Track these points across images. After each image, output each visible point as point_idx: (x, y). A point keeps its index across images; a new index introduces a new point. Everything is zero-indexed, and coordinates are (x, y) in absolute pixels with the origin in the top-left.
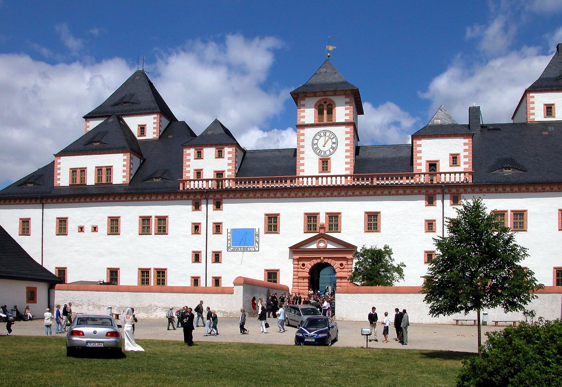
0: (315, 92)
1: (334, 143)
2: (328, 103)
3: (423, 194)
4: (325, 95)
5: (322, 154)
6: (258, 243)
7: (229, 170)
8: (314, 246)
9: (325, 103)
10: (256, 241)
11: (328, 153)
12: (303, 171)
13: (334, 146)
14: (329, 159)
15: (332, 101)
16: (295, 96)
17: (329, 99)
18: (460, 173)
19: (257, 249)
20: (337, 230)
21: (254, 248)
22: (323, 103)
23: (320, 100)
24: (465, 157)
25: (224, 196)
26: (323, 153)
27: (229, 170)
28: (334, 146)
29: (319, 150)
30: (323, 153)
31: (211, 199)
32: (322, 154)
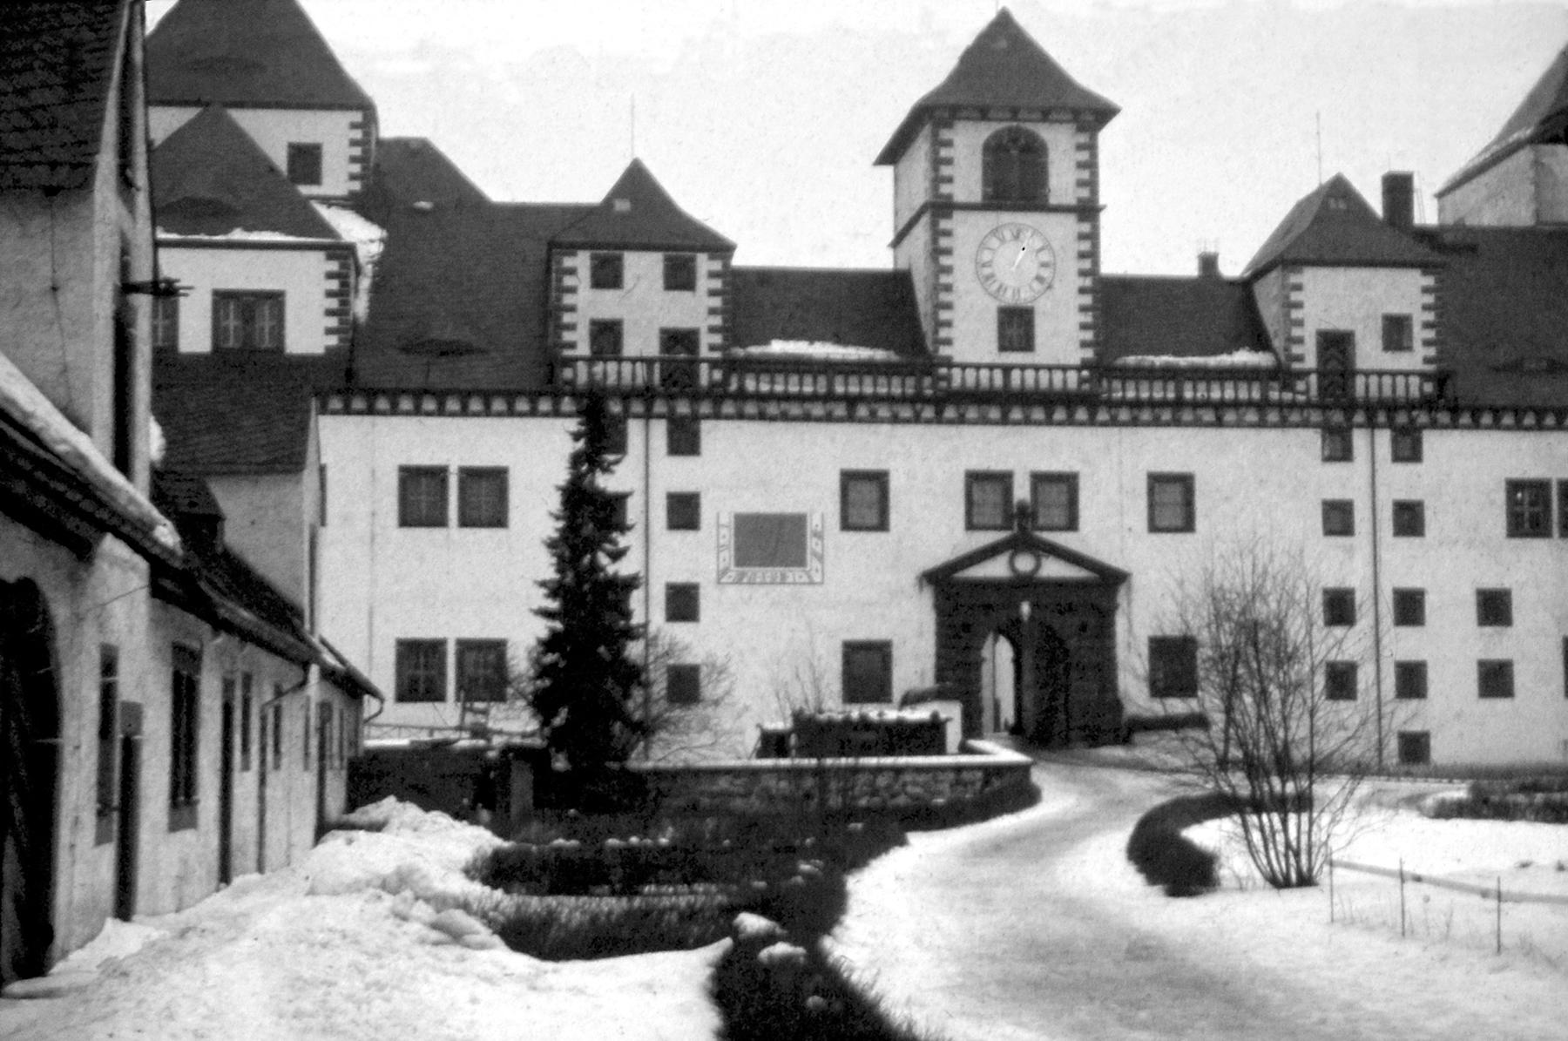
1: (1044, 265)
3: (1315, 426)
5: (1009, 294)
6: (821, 558)
7: (712, 330)
8: (996, 569)
10: (815, 554)
13: (1046, 273)
18: (1407, 374)
19: (817, 578)
20: (1072, 524)
21: (809, 577)
24: (1427, 325)
25: (705, 408)
27: (712, 330)
31: (660, 416)
32: (1009, 294)
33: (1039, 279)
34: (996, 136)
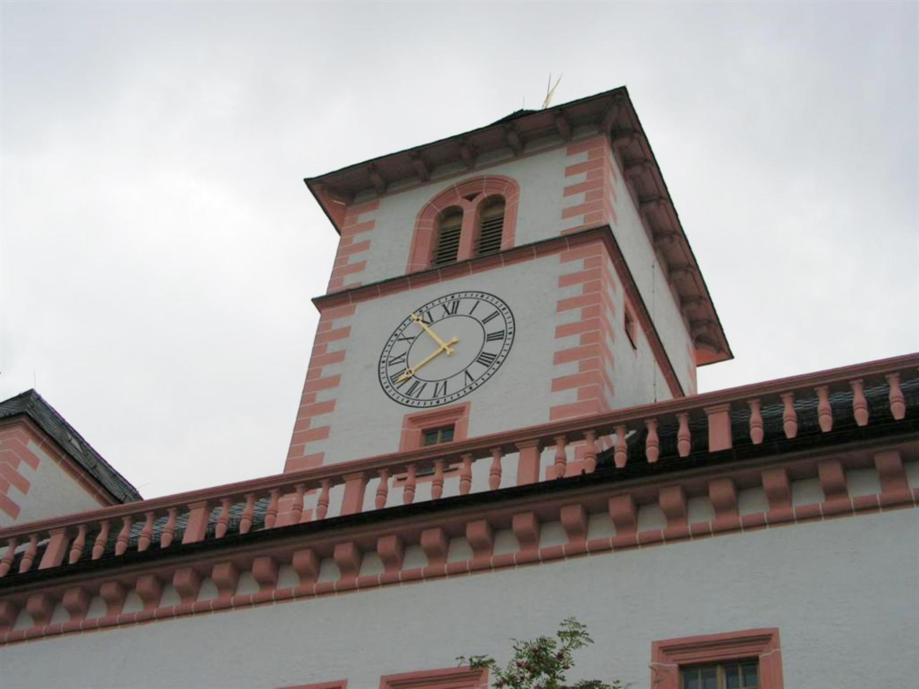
5: (428, 393)
11: (455, 386)
15: (503, 180)
17: (491, 179)
22: (459, 202)
28: (494, 347)
32: (428, 393)
33: (485, 359)
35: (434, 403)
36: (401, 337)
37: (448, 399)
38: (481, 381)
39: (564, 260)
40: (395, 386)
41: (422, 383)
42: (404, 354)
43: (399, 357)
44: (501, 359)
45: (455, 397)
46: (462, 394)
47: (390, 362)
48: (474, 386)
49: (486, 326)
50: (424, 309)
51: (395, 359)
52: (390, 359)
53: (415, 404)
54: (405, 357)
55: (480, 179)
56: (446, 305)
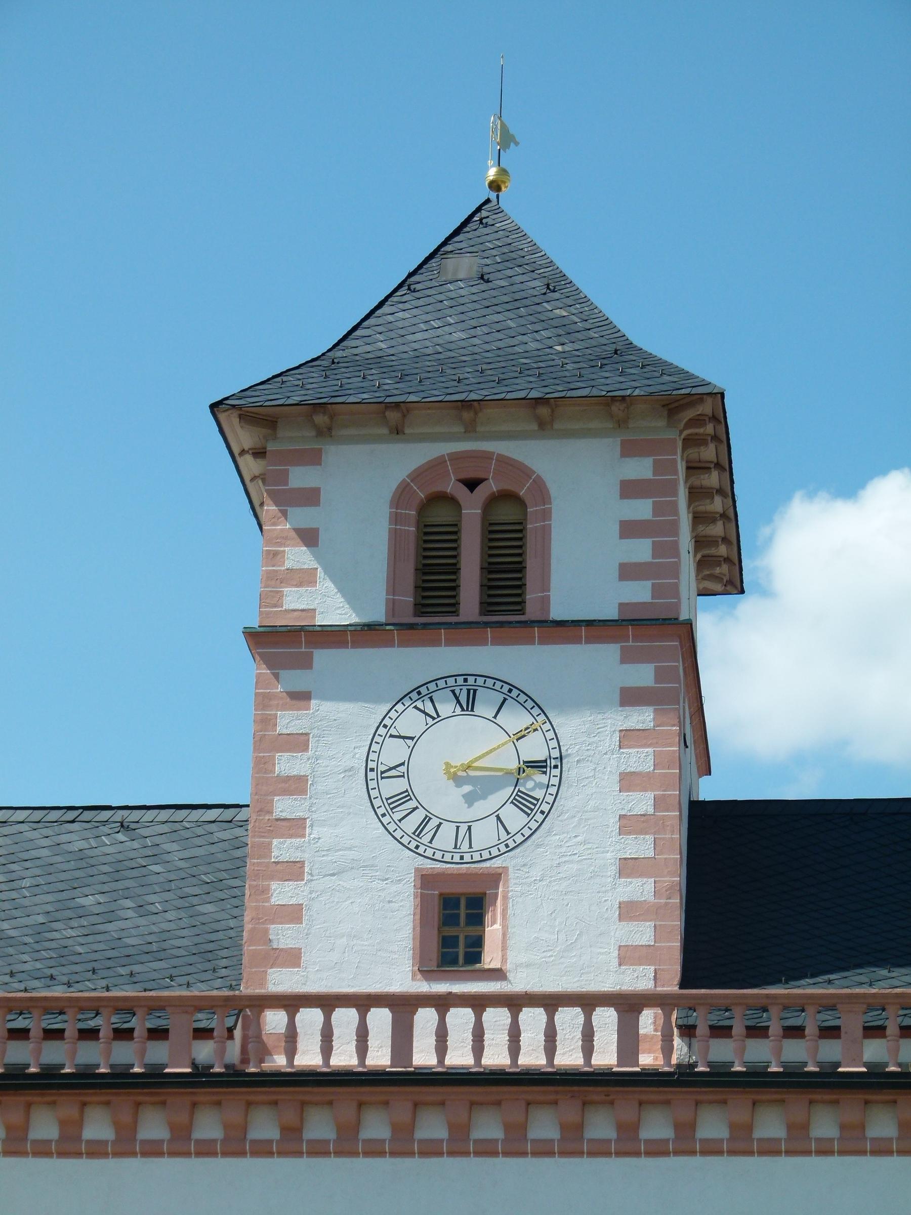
0: (397, 405)
2: (492, 486)
4: (470, 430)
5: (445, 839)
9: (472, 484)
12: (293, 958)
14: (495, 878)
15: (524, 472)
16: (245, 437)
17: (505, 462)
22: (452, 486)
23: (437, 465)
26: (448, 831)
29: (419, 816)
30: (448, 831)
32: (445, 839)
34: (418, 475)
35: (457, 859)
36: (393, 732)
37: (477, 857)
38: (518, 839)
39: (627, 658)
40: (397, 817)
41: (434, 822)
42: (403, 764)
43: (394, 768)
44: (545, 807)
45: (486, 855)
46: (495, 852)
47: (382, 773)
48: (512, 845)
49: (519, 744)
50: (423, 690)
51: (391, 769)
52: (382, 768)
53: (429, 853)
54: (403, 769)
55: (486, 456)
56: (457, 692)
